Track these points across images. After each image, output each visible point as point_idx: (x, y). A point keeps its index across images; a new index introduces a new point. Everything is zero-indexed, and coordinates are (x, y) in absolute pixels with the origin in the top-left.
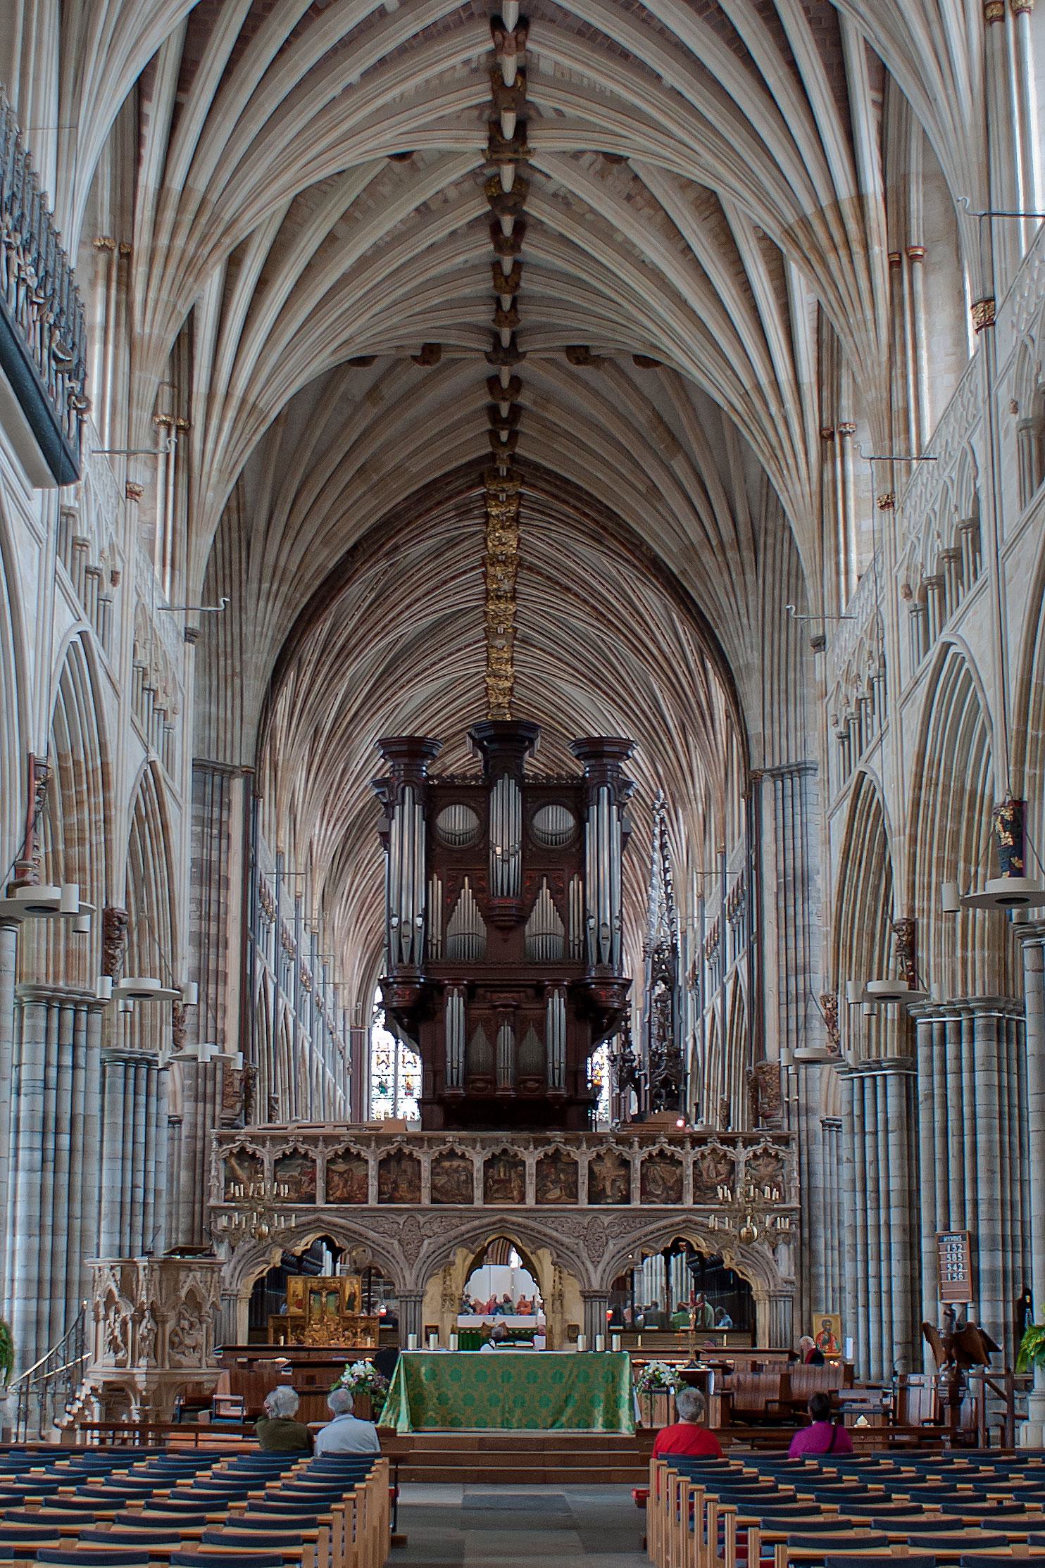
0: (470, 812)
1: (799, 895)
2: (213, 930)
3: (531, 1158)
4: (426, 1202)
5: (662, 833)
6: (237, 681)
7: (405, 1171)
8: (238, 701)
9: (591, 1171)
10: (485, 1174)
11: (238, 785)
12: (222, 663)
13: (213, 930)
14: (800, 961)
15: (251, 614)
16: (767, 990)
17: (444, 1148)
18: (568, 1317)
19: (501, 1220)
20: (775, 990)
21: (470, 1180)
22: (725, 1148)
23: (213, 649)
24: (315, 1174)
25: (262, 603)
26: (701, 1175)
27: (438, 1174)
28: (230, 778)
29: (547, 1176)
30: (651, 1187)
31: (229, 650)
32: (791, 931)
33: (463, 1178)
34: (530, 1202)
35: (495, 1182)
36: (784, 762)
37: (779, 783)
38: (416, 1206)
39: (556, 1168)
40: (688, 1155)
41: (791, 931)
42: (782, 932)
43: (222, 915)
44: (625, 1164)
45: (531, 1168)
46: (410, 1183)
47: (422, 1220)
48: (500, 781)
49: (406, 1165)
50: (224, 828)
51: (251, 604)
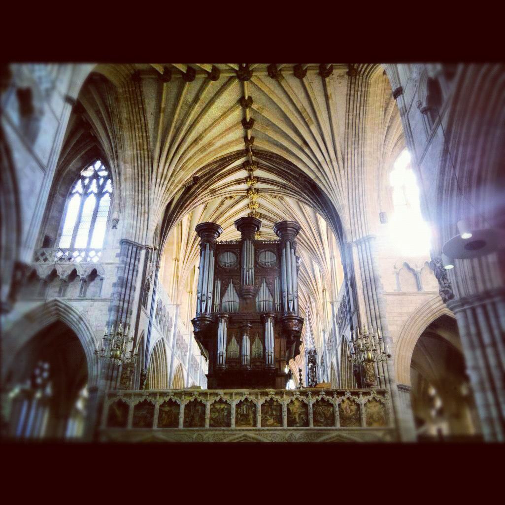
2: (126, 305)
3: (260, 401)
4: (207, 426)
5: (309, 315)
6: (146, 215)
8: (146, 222)
9: (288, 409)
10: (236, 411)
11: (143, 252)
12: (140, 206)
13: (126, 305)
14: (378, 314)
15: (153, 190)
17: (218, 399)
19: (244, 436)
21: (229, 413)
22: (353, 397)
23: (136, 201)
25: (157, 186)
26: (343, 412)
27: (214, 412)
29: (267, 413)
30: (318, 418)
31: (143, 203)
32: (371, 302)
33: (226, 414)
34: (259, 426)
36: (361, 237)
37: (359, 247)
38: (201, 428)
39: (271, 408)
40: (336, 401)
41: (371, 302)
42: (367, 303)
44: (305, 405)
45: (259, 409)
48: (246, 242)
49: (199, 408)
50: (136, 267)
51: (153, 187)
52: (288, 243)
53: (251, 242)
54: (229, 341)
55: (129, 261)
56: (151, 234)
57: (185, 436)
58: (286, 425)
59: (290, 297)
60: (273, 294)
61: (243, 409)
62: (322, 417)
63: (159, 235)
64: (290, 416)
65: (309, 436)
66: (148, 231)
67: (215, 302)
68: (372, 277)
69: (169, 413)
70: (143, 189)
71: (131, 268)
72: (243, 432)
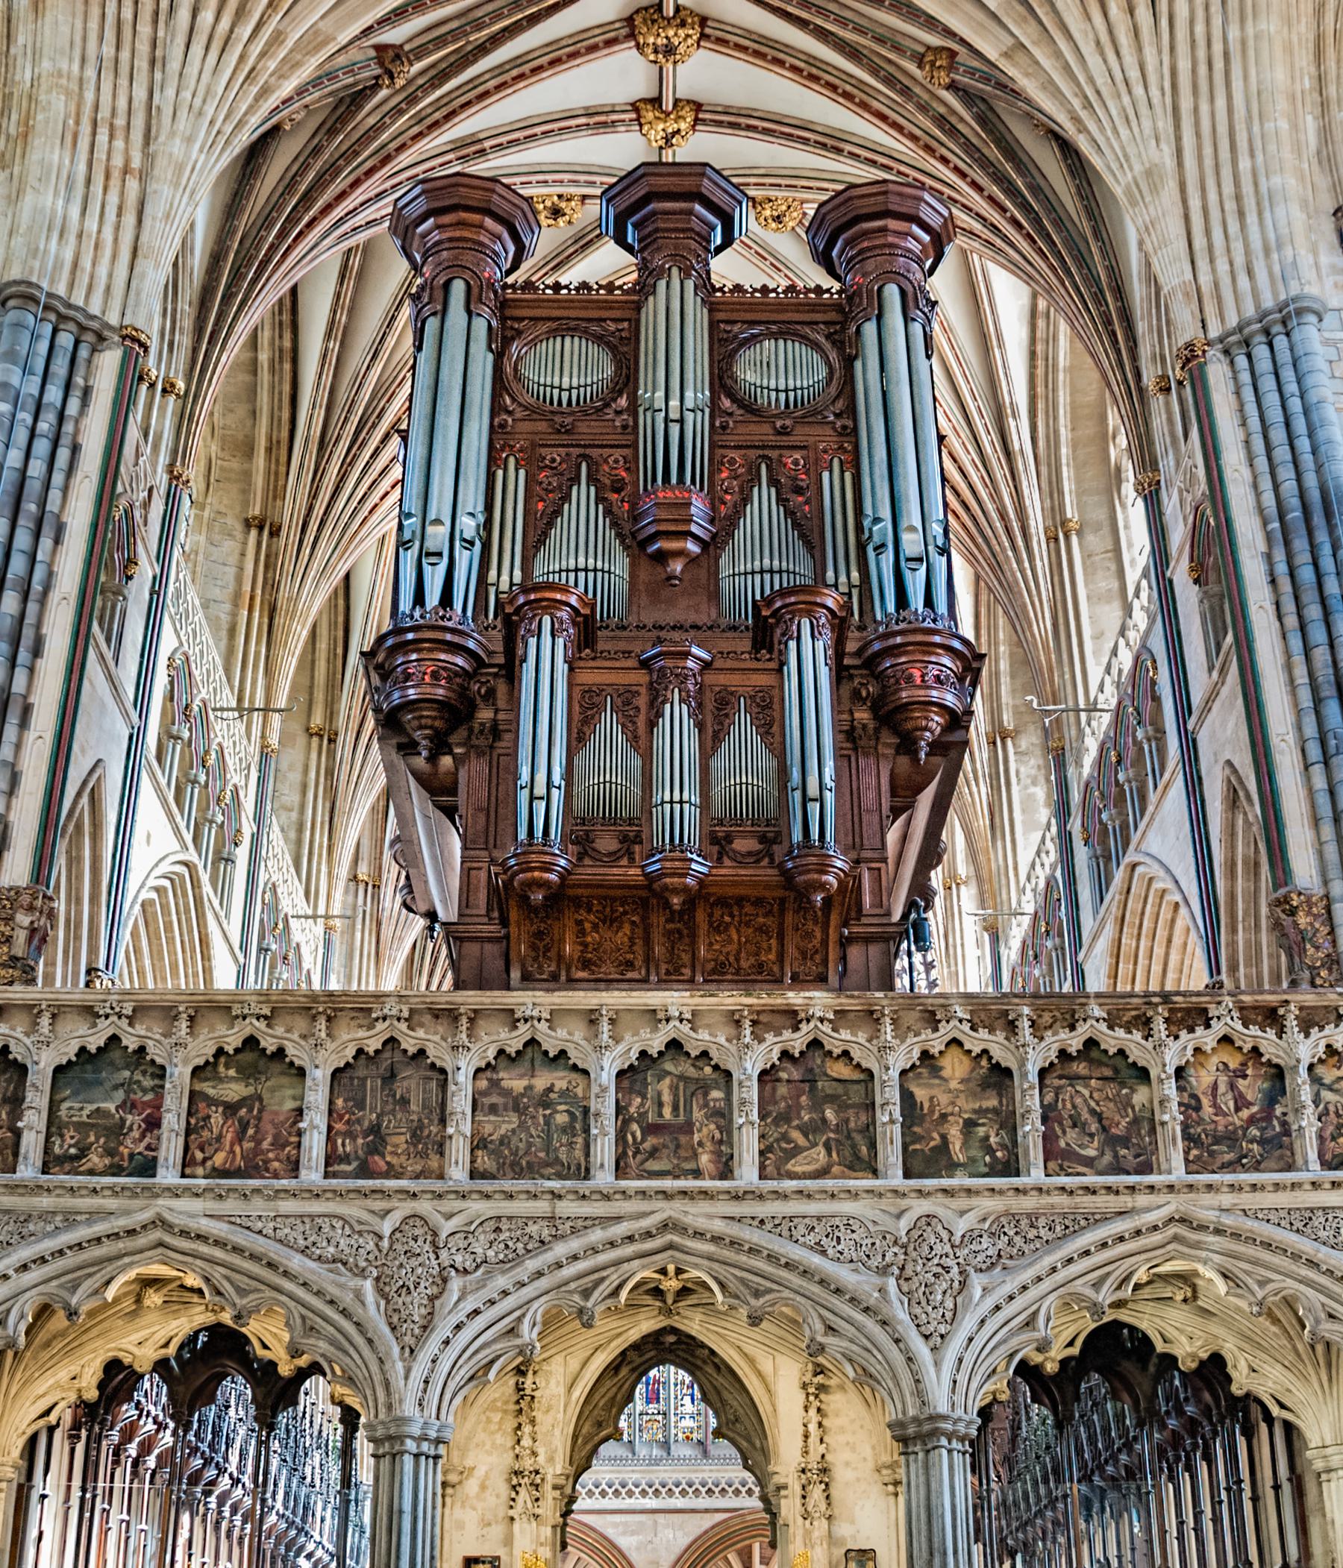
0: (593, 349)
1: (1322, 537)
4: (458, 1174)
6: (133, 185)
7: (404, 1102)
8: (130, 219)
9: (907, 1098)
10: (619, 1109)
12: (103, 137)
15: (174, 65)
16: (1275, 741)
18: (843, 1530)
19: (665, 1226)
20: (1291, 738)
24: (157, 1105)
26: (1198, 1108)
27: (493, 1109)
28: (94, 350)
30: (1069, 1138)
31: (120, 122)
33: (561, 1119)
34: (747, 1173)
35: (650, 1129)
41: (1314, 612)
42: (1292, 621)
43: (37, 587)
44: (999, 1076)
46: (416, 1134)
47: (447, 1227)
48: (662, 285)
49: (410, 1082)
50: (68, 428)
52: (892, 292)
53: (690, 285)
54: (578, 737)
55: (33, 386)
56: (155, 276)
57: (339, 1224)
58: (900, 1173)
59: (912, 544)
60: (816, 541)
61: (659, 1094)
62: (1092, 1135)
63: (187, 323)
64: (916, 1129)
65: (1024, 1222)
66: (139, 261)
67: (493, 574)
68: (1315, 495)
69: (243, 1112)
70: (125, 55)
71: (43, 426)
72: (659, 1204)
